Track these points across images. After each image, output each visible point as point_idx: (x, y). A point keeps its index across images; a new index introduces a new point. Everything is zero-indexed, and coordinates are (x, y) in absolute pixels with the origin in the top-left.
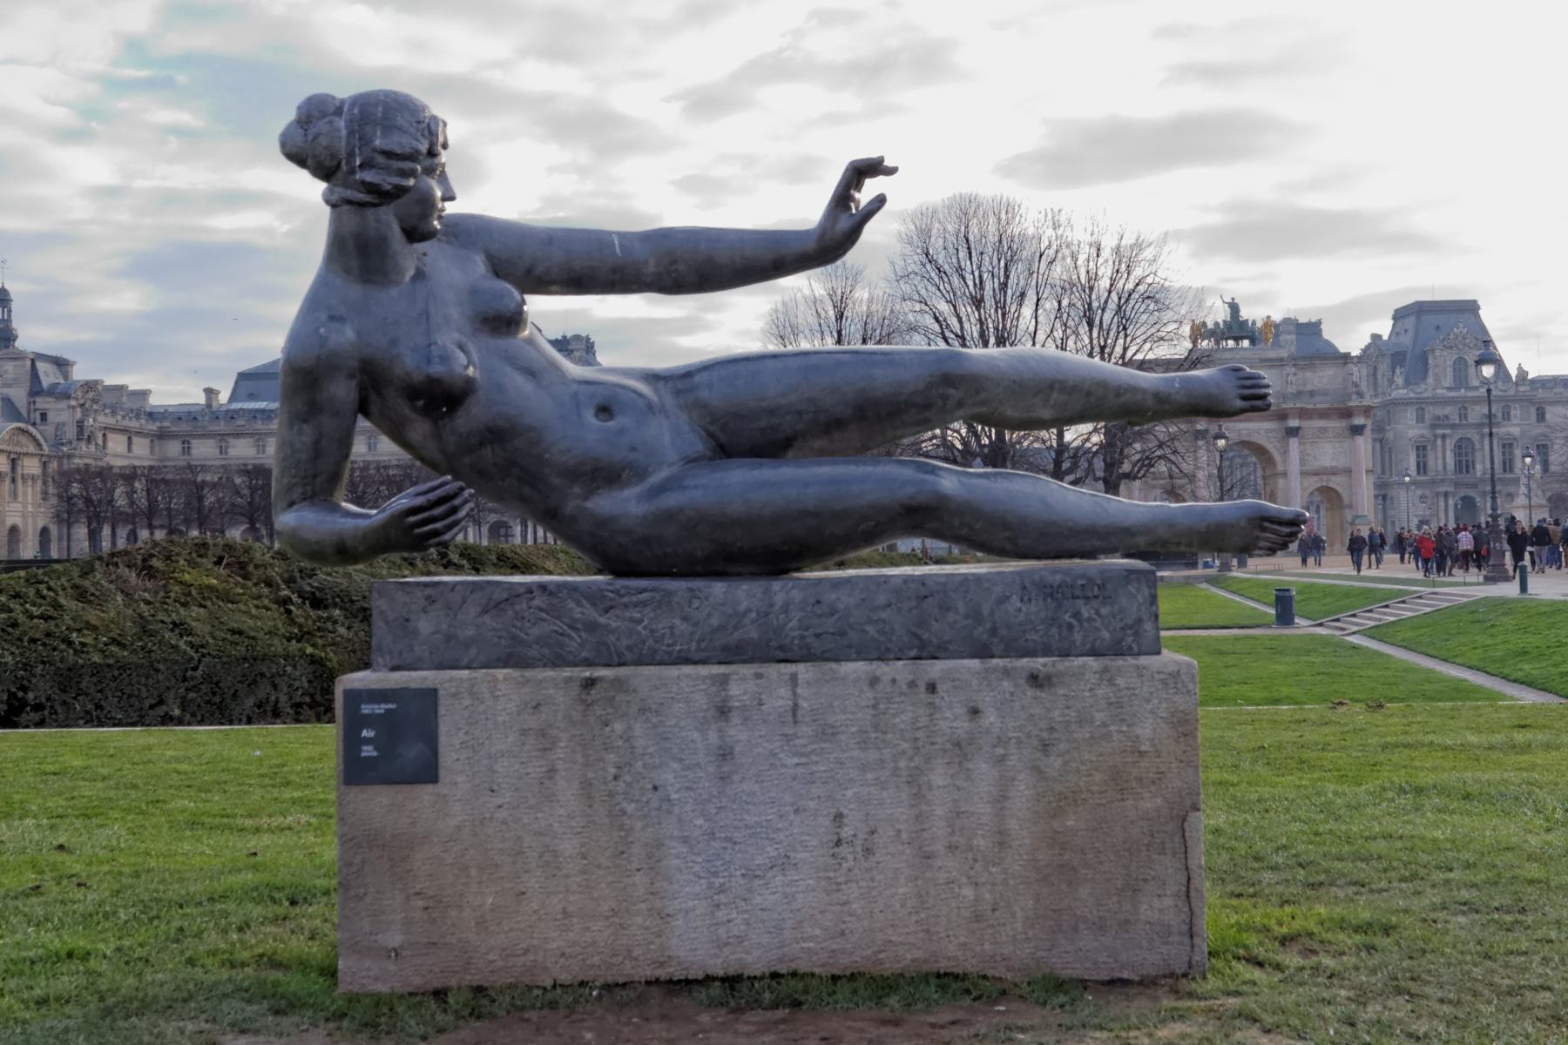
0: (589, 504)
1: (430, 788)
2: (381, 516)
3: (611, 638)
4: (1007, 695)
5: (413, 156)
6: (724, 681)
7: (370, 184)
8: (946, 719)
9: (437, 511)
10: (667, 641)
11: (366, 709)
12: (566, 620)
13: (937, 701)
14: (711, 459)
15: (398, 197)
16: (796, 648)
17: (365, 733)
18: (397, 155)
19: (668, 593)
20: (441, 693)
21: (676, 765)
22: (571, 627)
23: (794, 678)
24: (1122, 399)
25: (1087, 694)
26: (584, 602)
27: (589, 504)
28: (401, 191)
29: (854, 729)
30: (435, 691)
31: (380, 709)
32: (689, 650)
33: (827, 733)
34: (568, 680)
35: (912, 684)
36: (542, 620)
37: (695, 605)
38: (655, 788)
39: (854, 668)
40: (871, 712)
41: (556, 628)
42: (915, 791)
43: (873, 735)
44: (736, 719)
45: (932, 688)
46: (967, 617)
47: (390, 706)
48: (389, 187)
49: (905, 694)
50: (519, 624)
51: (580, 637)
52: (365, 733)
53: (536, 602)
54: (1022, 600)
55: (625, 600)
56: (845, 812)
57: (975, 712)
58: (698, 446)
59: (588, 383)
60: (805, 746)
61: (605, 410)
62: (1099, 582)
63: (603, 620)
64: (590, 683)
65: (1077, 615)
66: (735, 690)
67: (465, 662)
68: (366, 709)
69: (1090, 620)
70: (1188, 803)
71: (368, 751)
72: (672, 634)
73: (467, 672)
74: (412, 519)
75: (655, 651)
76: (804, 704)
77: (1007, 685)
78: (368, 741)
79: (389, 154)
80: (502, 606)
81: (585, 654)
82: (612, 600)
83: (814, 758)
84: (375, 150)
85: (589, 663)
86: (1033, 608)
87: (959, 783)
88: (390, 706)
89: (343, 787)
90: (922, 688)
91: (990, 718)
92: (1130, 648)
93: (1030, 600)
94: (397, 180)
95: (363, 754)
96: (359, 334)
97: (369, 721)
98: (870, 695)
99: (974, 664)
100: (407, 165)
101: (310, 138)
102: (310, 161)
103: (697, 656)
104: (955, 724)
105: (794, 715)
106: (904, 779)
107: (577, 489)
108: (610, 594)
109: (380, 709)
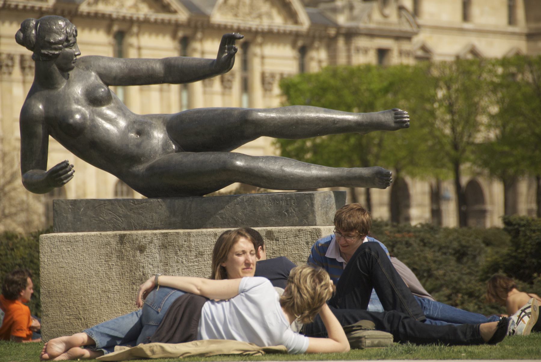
3: (132, 221)
5: (60, 42)
7: (44, 54)
9: (61, 172)
12: (118, 214)
21: (151, 266)
24: (337, 125)
27: (130, 170)
28: (58, 55)
32: (158, 224)
36: (110, 214)
37: (160, 208)
41: (114, 217)
46: (251, 212)
48: (51, 55)
51: (122, 220)
55: (137, 206)
63: (128, 213)
64: (122, 237)
81: (123, 226)
82: (132, 206)
83: (196, 264)
108: (132, 204)
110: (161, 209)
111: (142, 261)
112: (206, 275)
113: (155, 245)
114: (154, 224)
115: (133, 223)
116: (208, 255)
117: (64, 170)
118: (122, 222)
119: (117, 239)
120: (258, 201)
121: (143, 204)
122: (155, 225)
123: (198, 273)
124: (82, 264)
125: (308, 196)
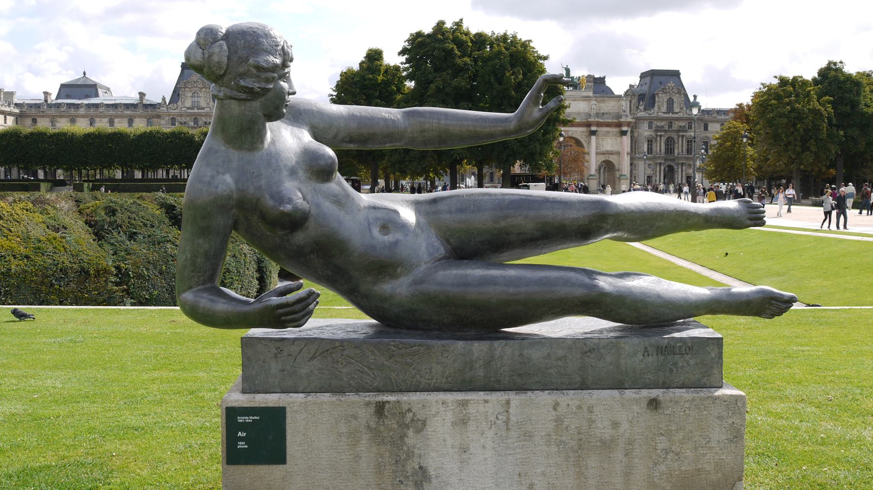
0: (376, 288)
1: (281, 467)
2: (258, 306)
3: (393, 375)
4: (636, 414)
6: (464, 404)
8: (598, 428)
10: (427, 377)
11: (240, 419)
12: (365, 364)
13: (593, 417)
14: (448, 258)
15: (264, 95)
16: (506, 382)
17: (240, 434)
18: (264, 68)
19: (429, 347)
20: (288, 410)
22: (368, 368)
23: (508, 402)
25: (682, 414)
26: (375, 351)
28: (265, 91)
29: (543, 434)
30: (284, 408)
31: (249, 419)
32: (441, 382)
33: (528, 436)
34: (368, 404)
35: (579, 407)
38: (421, 468)
39: (545, 398)
40: (554, 424)
42: (577, 470)
43: (554, 437)
44: (472, 425)
45: (590, 410)
47: (256, 418)
49: (575, 413)
50: (335, 365)
51: (374, 374)
52: (240, 434)
53: (346, 352)
54: (643, 355)
55: (402, 351)
56: (536, 482)
57: (615, 425)
58: (442, 251)
59: (375, 208)
60: (513, 443)
61: (385, 228)
62: (689, 345)
65: (675, 364)
66: (472, 409)
67: (301, 389)
68: (240, 419)
69: (682, 367)
70: (736, 476)
71: (242, 445)
72: (431, 372)
73: (302, 395)
74: (280, 311)
75: (420, 382)
76: (513, 418)
77: (636, 408)
78: (241, 439)
79: (259, 68)
80: (325, 354)
82: (393, 351)
83: (518, 451)
84: (249, 65)
85: (379, 390)
86: (650, 359)
87: (605, 465)
88: (256, 418)
89: (226, 466)
90: (586, 409)
91: (625, 426)
92: (705, 383)
93: (648, 355)
94: (263, 85)
95: (238, 447)
96: (237, 181)
97: (244, 426)
98: (554, 413)
99: (615, 393)
100: (270, 75)
101: (206, 56)
102: (205, 70)
103: (446, 386)
104: (603, 431)
105: (507, 425)
106: (572, 463)
107: (369, 279)
108: (392, 347)
109: (249, 419)
110: (447, 357)
111: (418, 446)
112: (537, 468)
113: (444, 419)
114: (433, 381)
115: (395, 379)
116: (542, 436)
117: (304, 303)
118: (372, 378)
119: (372, 410)
120: (624, 348)
121: (414, 348)
122: (435, 382)
123: (523, 465)
124: (304, 450)
125: (713, 341)
